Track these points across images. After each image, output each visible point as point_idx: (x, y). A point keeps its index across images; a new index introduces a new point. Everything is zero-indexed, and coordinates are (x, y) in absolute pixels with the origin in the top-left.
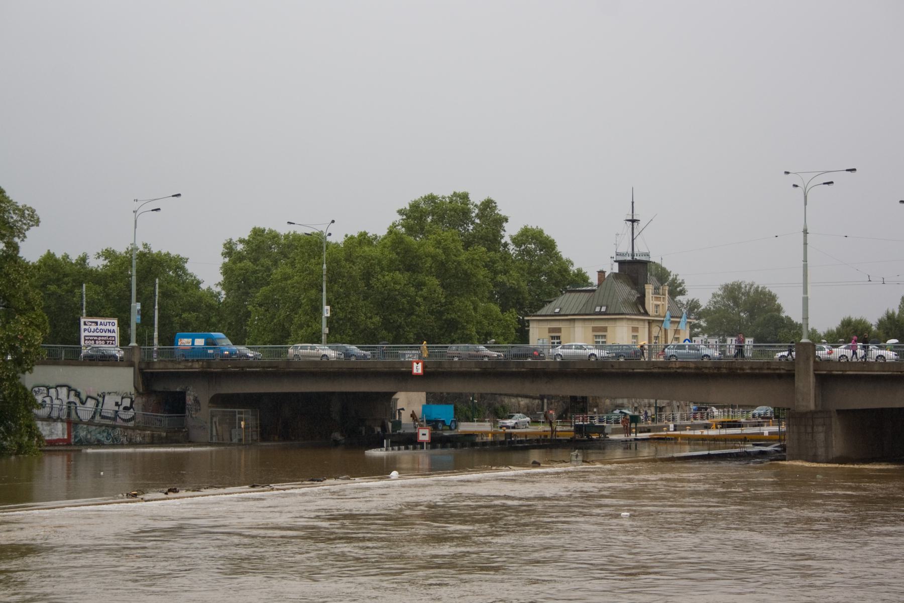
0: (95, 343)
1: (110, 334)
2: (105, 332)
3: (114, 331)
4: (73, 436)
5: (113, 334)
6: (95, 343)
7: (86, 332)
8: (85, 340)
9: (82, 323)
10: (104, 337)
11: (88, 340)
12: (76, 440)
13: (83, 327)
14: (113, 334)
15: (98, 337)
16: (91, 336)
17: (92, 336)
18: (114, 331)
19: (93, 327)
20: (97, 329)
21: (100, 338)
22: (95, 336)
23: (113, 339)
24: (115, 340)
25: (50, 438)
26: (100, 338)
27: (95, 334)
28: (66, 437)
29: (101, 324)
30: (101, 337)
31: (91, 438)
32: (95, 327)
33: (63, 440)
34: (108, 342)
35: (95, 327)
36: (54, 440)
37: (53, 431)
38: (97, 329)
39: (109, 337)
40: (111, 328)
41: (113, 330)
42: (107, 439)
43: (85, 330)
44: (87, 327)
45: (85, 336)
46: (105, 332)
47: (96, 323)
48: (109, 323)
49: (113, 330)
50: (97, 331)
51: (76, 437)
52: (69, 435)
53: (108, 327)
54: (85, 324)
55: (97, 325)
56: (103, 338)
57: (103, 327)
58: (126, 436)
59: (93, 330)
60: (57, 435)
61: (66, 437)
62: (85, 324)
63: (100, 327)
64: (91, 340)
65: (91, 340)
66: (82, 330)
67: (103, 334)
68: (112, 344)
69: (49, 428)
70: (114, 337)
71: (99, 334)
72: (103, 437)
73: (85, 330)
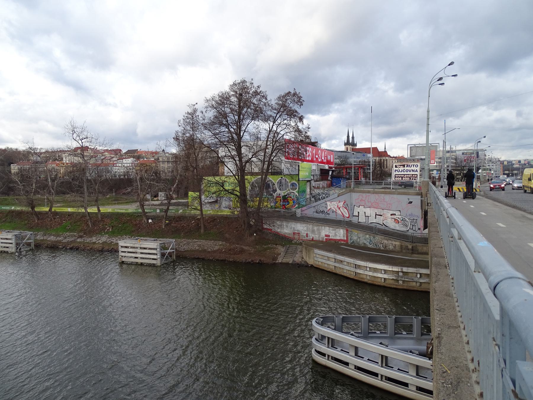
0: (402, 179)
1: (413, 173)
2: (410, 172)
3: (417, 171)
4: (349, 239)
5: (416, 173)
6: (402, 179)
7: (397, 172)
8: (395, 177)
9: (394, 166)
10: (409, 175)
11: (397, 177)
12: (351, 242)
13: (395, 168)
14: (416, 173)
15: (404, 175)
16: (399, 175)
17: (400, 175)
18: (417, 171)
19: (402, 168)
20: (404, 170)
21: (405, 176)
22: (402, 175)
23: (416, 176)
24: (417, 177)
25: (335, 238)
26: (405, 176)
27: (403, 173)
28: (345, 239)
29: (407, 166)
30: (407, 175)
31: (360, 241)
32: (403, 169)
33: (344, 240)
34: (412, 178)
35: (403, 169)
36: (337, 240)
37: (337, 234)
38: (404, 170)
39: (412, 175)
40: (415, 168)
41: (417, 170)
42: (370, 244)
43: (396, 171)
44: (397, 169)
45: (395, 175)
46: (410, 172)
47: (404, 166)
48: (414, 165)
49: (417, 170)
50: (404, 171)
51: (351, 239)
52: (347, 237)
53: (412, 168)
54: (396, 167)
55: (404, 167)
56: (408, 176)
57: (408, 168)
58: (383, 244)
59: (401, 171)
60: (340, 236)
61: (345, 239)
62: (396, 167)
63: (406, 168)
64: (399, 177)
65: (399, 177)
66: (419, 171)
67: (409, 173)
68: (415, 179)
69: (334, 232)
70: (417, 175)
71: (406, 173)
72: (367, 242)
73: (396, 171)
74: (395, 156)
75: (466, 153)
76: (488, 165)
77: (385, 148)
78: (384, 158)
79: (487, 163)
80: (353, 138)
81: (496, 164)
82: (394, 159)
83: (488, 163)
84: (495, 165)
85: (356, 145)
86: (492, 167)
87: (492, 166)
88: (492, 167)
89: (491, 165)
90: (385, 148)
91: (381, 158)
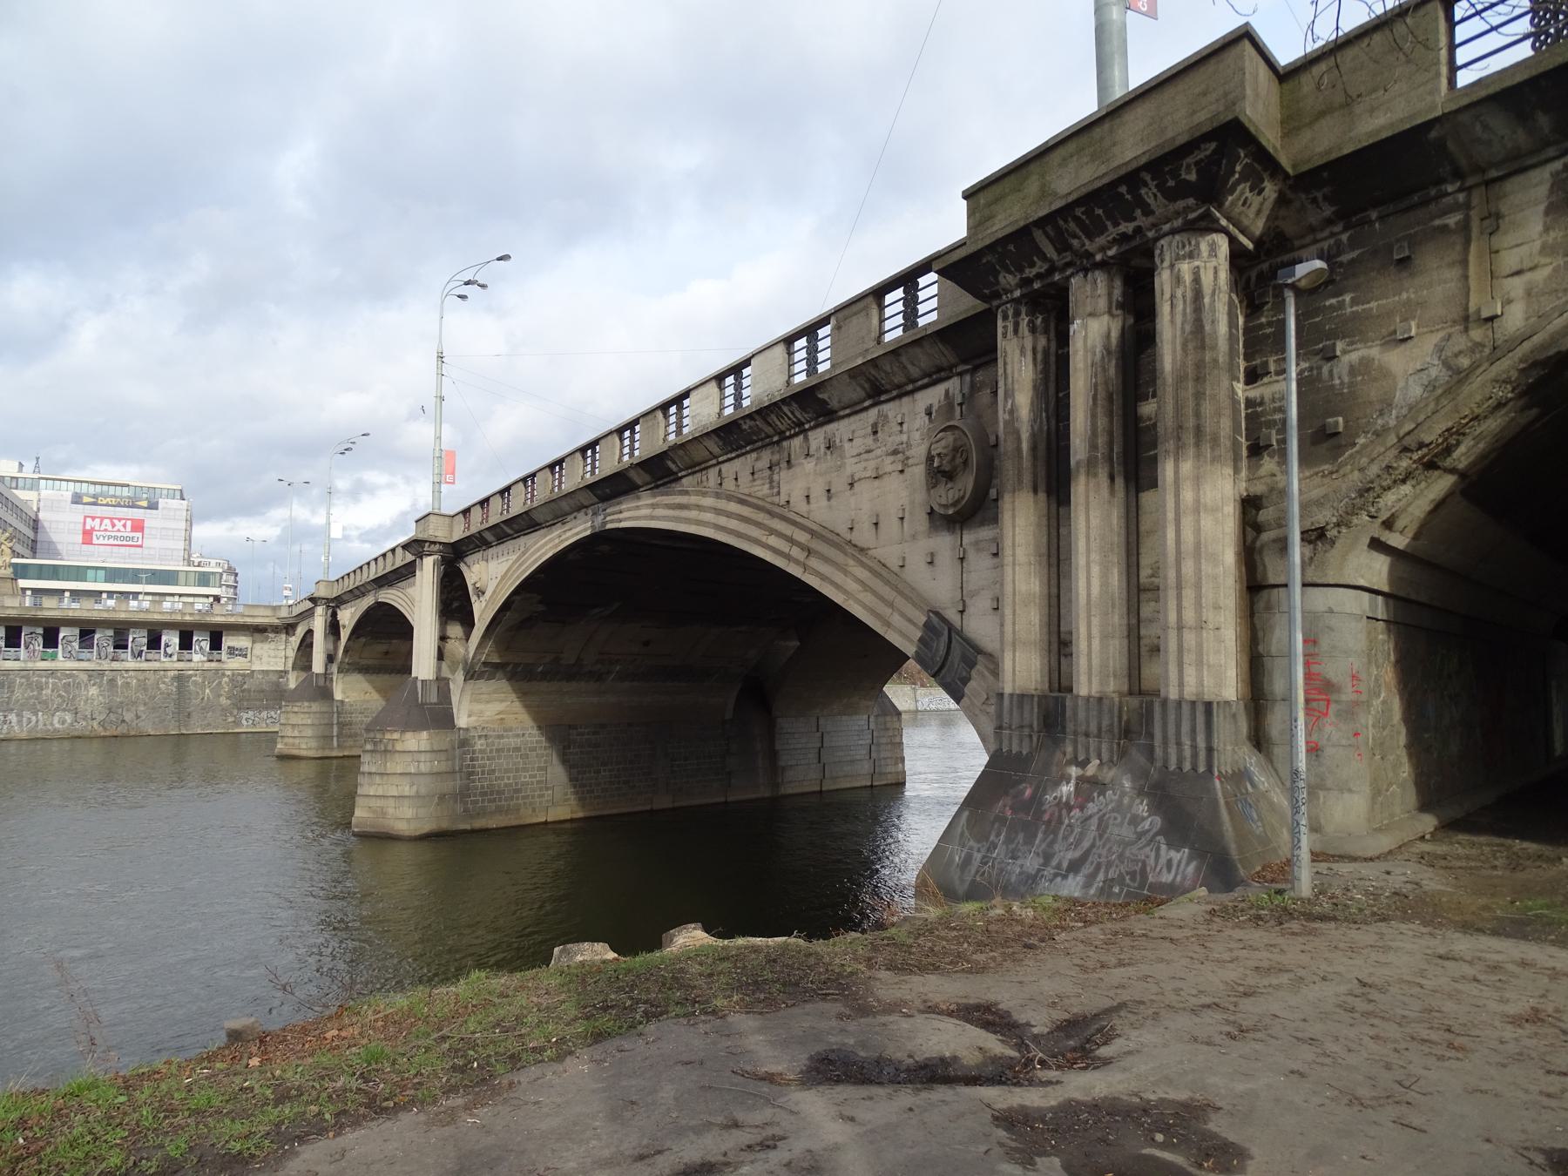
75: (95, 496)
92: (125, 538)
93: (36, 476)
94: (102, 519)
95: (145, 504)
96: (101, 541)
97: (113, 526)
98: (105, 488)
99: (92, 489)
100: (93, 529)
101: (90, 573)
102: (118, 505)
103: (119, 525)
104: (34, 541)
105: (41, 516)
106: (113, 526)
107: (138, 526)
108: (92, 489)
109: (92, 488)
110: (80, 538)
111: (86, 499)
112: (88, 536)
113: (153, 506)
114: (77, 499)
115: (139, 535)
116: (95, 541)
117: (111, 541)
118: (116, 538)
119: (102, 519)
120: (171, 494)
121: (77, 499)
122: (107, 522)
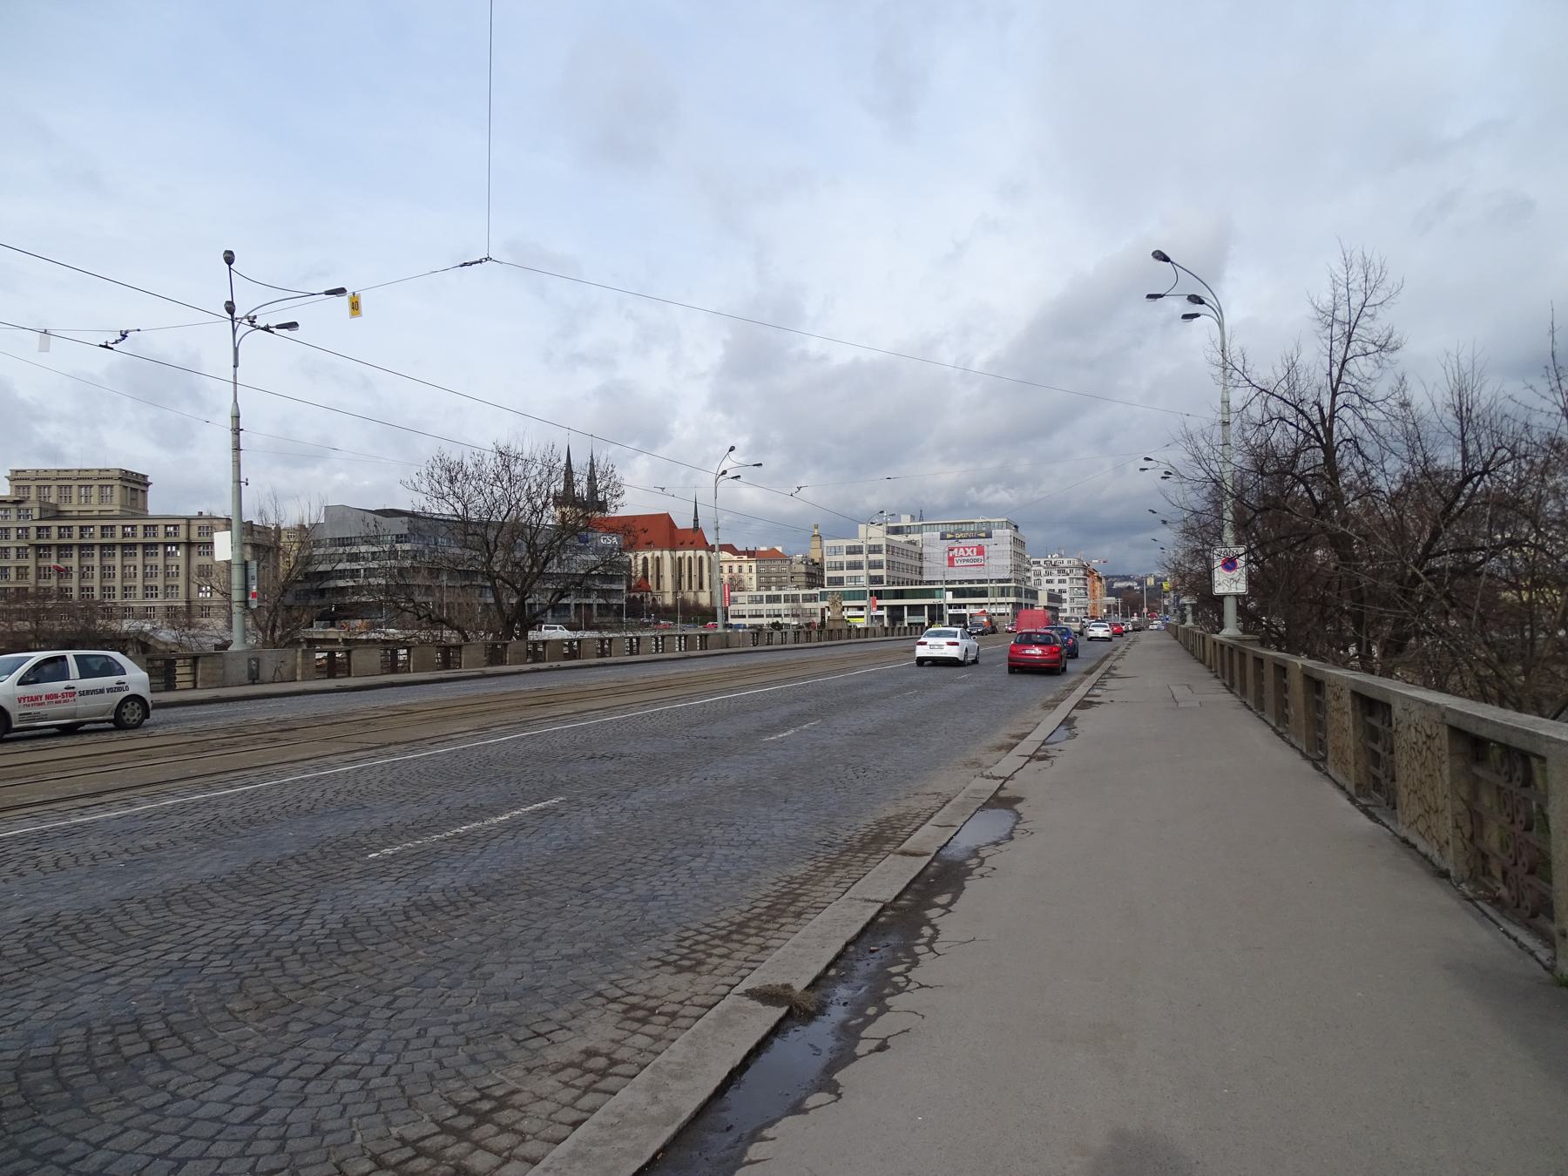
74: (751, 548)
76: (1049, 578)
77: (696, 520)
78: (690, 553)
79: (1043, 572)
80: (592, 479)
81: (1071, 575)
82: (745, 558)
83: (1048, 574)
84: (1067, 578)
85: (602, 507)
86: (1062, 586)
87: (1060, 581)
88: (1062, 586)
89: (1056, 579)
90: (696, 520)
91: (679, 554)
92: (974, 560)
93: (920, 523)
94: (959, 548)
95: (983, 535)
96: (959, 564)
97: (966, 552)
98: (960, 526)
99: (952, 528)
100: (954, 556)
101: (937, 593)
102: (968, 538)
103: (969, 551)
104: (921, 568)
105: (924, 550)
106: (966, 552)
107: (981, 551)
108: (952, 528)
109: (952, 527)
110: (947, 563)
111: (949, 536)
112: (951, 559)
113: (989, 536)
114: (943, 537)
115: (981, 557)
116: (956, 564)
117: (965, 563)
118: (967, 561)
119: (959, 548)
120: (1000, 526)
121: (943, 537)
122: (962, 550)
